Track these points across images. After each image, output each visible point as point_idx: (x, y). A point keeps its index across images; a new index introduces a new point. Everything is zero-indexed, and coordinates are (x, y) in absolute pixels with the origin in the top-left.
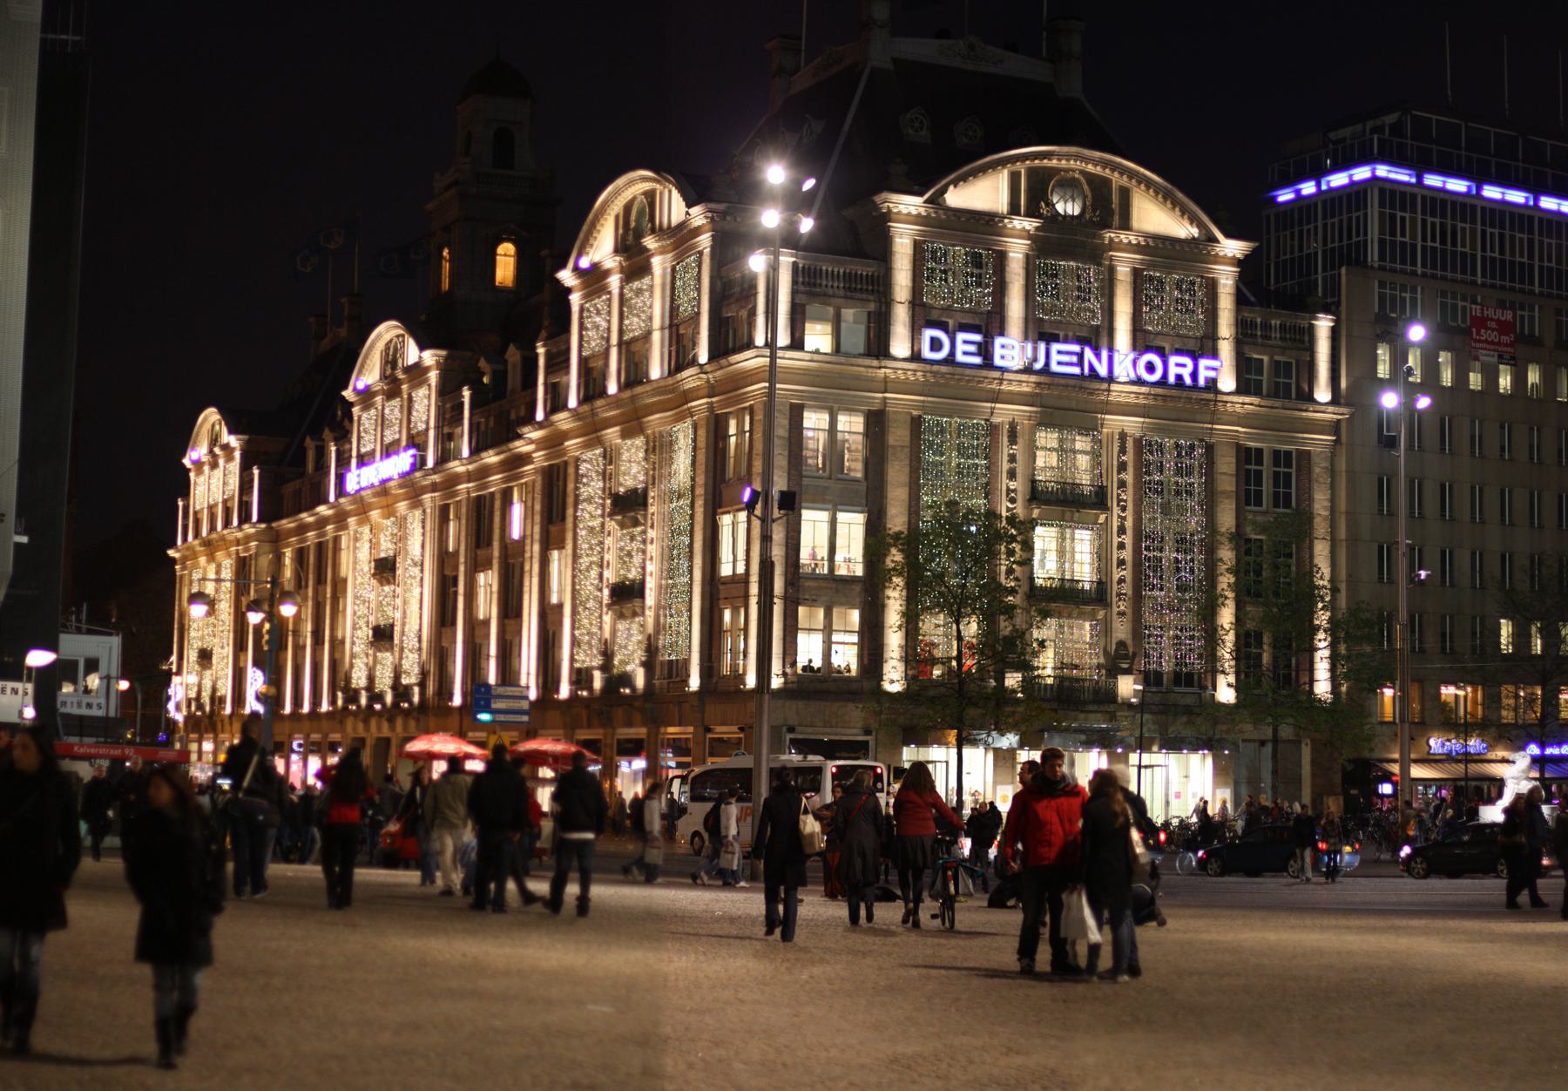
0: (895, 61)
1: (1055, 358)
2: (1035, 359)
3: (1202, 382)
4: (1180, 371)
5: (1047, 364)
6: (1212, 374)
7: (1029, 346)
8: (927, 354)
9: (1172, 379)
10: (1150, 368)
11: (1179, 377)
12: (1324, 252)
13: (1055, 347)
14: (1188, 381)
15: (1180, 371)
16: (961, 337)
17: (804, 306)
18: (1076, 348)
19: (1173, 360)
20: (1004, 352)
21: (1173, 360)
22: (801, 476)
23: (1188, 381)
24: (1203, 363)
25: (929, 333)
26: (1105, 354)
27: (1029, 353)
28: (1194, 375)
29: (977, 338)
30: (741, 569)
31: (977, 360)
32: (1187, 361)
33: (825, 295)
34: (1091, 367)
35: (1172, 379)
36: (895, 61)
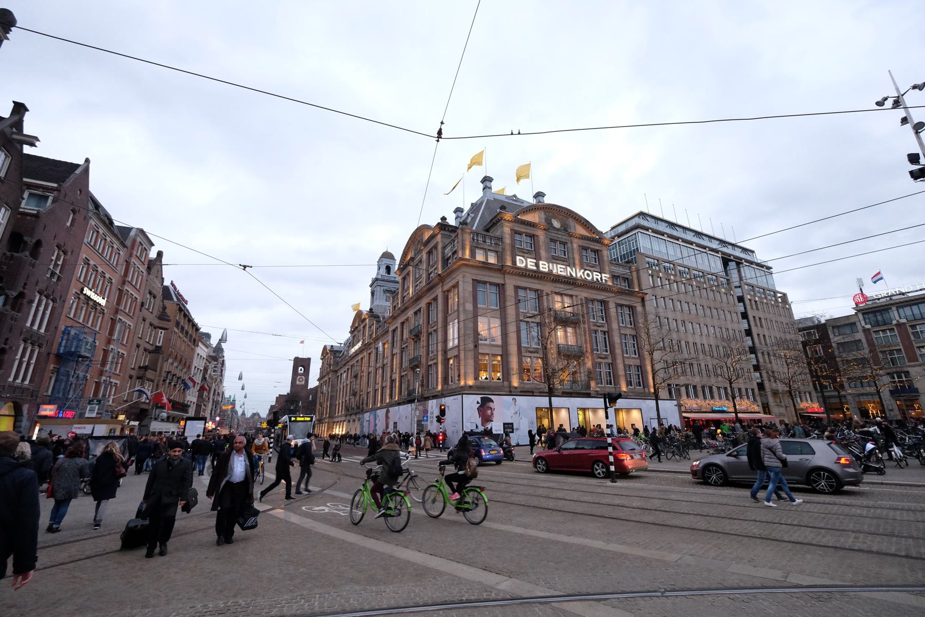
1: (559, 269)
3: (604, 281)
4: (597, 277)
8: (518, 264)
9: (595, 280)
10: (588, 275)
12: (621, 256)
13: (559, 266)
14: (599, 280)
15: (597, 277)
16: (529, 260)
18: (564, 267)
20: (544, 266)
21: (595, 273)
24: (603, 275)
26: (574, 269)
28: (601, 278)
29: (534, 261)
30: (456, 342)
31: (535, 268)
35: (595, 280)
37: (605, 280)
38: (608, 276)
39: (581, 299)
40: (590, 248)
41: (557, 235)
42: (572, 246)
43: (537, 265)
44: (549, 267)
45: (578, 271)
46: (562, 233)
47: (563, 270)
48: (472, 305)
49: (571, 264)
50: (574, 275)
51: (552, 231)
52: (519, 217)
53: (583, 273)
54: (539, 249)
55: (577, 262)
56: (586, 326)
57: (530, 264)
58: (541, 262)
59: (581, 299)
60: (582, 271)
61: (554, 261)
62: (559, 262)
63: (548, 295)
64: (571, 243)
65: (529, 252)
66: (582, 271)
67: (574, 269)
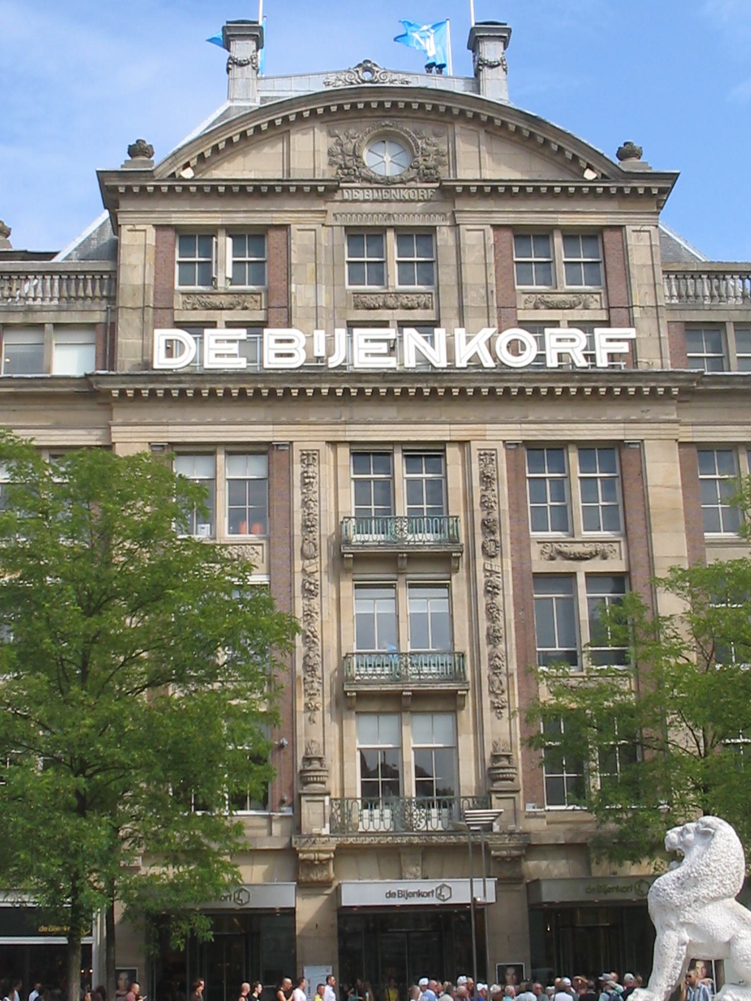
2: (330, 351)
3: (602, 362)
4: (564, 347)
6: (625, 348)
7: (320, 336)
8: (161, 361)
10: (515, 347)
18: (391, 333)
20: (285, 348)
21: (550, 333)
24: (601, 333)
25: (161, 336)
29: (242, 333)
31: (241, 363)
32: (577, 333)
35: (552, 362)
37: (611, 356)
38: (631, 333)
39: (487, 456)
40: (557, 227)
41: (384, 207)
43: (252, 348)
44: (308, 348)
46: (405, 194)
49: (450, 314)
50: (439, 360)
51: (360, 195)
52: (188, 174)
53: (490, 345)
56: (506, 565)
58: (270, 335)
60: (488, 332)
63: (309, 457)
64: (456, 226)
65: (239, 300)
66: (488, 332)
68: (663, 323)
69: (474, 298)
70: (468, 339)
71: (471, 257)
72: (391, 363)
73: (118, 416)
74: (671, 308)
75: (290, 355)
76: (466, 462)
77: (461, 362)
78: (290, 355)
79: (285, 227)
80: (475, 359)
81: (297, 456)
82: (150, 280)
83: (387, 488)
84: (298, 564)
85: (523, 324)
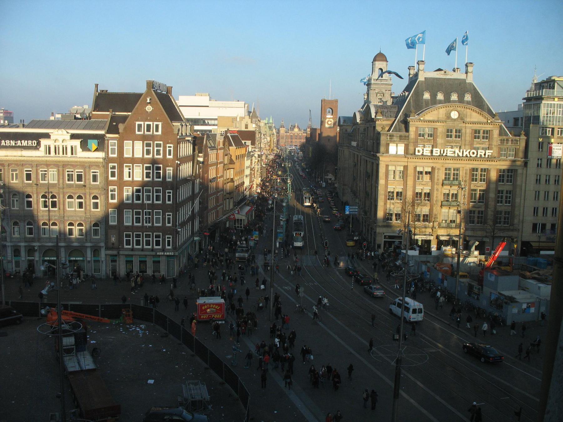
0: (425, 78)
1: (448, 152)
2: (444, 153)
3: (487, 156)
4: (481, 154)
5: (447, 153)
6: (490, 154)
8: (417, 153)
9: (479, 156)
10: (473, 153)
11: (481, 155)
14: (483, 156)
17: (389, 144)
19: (479, 151)
20: (437, 152)
22: (388, 180)
23: (483, 156)
24: (487, 151)
27: (442, 152)
28: (485, 155)
32: (484, 152)
33: (394, 141)
34: (458, 154)
35: (479, 156)
36: (425, 78)
37: (488, 155)
38: (492, 151)
39: (466, 170)
42: (466, 131)
44: (440, 152)
45: (465, 151)
47: (452, 152)
48: (384, 181)
50: (461, 154)
51: (449, 122)
52: (422, 119)
53: (469, 153)
54: (437, 137)
55: (467, 142)
57: (427, 152)
59: (466, 170)
61: (448, 144)
62: (452, 144)
63: (439, 169)
66: (469, 151)
67: (461, 151)
68: (497, 148)
69: (467, 142)
70: (466, 151)
71: (467, 135)
72: (453, 155)
73: (409, 160)
74: (499, 145)
75: (437, 153)
76: (463, 171)
77: (464, 155)
78: (437, 153)
79: (437, 128)
80: (467, 155)
81: (436, 169)
82: (414, 137)
83: (449, 174)
84: (436, 186)
85: (474, 149)
